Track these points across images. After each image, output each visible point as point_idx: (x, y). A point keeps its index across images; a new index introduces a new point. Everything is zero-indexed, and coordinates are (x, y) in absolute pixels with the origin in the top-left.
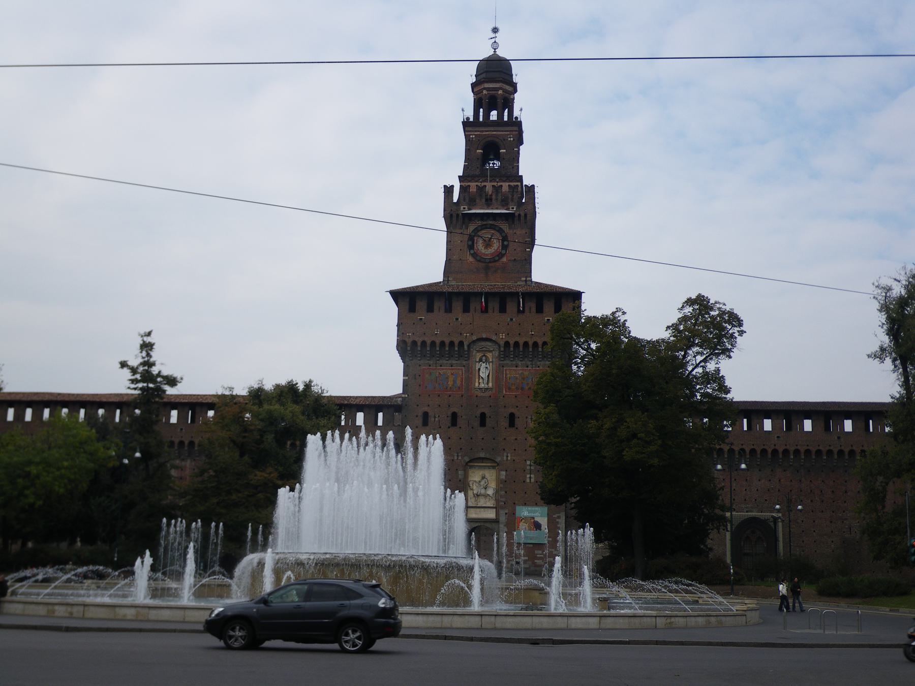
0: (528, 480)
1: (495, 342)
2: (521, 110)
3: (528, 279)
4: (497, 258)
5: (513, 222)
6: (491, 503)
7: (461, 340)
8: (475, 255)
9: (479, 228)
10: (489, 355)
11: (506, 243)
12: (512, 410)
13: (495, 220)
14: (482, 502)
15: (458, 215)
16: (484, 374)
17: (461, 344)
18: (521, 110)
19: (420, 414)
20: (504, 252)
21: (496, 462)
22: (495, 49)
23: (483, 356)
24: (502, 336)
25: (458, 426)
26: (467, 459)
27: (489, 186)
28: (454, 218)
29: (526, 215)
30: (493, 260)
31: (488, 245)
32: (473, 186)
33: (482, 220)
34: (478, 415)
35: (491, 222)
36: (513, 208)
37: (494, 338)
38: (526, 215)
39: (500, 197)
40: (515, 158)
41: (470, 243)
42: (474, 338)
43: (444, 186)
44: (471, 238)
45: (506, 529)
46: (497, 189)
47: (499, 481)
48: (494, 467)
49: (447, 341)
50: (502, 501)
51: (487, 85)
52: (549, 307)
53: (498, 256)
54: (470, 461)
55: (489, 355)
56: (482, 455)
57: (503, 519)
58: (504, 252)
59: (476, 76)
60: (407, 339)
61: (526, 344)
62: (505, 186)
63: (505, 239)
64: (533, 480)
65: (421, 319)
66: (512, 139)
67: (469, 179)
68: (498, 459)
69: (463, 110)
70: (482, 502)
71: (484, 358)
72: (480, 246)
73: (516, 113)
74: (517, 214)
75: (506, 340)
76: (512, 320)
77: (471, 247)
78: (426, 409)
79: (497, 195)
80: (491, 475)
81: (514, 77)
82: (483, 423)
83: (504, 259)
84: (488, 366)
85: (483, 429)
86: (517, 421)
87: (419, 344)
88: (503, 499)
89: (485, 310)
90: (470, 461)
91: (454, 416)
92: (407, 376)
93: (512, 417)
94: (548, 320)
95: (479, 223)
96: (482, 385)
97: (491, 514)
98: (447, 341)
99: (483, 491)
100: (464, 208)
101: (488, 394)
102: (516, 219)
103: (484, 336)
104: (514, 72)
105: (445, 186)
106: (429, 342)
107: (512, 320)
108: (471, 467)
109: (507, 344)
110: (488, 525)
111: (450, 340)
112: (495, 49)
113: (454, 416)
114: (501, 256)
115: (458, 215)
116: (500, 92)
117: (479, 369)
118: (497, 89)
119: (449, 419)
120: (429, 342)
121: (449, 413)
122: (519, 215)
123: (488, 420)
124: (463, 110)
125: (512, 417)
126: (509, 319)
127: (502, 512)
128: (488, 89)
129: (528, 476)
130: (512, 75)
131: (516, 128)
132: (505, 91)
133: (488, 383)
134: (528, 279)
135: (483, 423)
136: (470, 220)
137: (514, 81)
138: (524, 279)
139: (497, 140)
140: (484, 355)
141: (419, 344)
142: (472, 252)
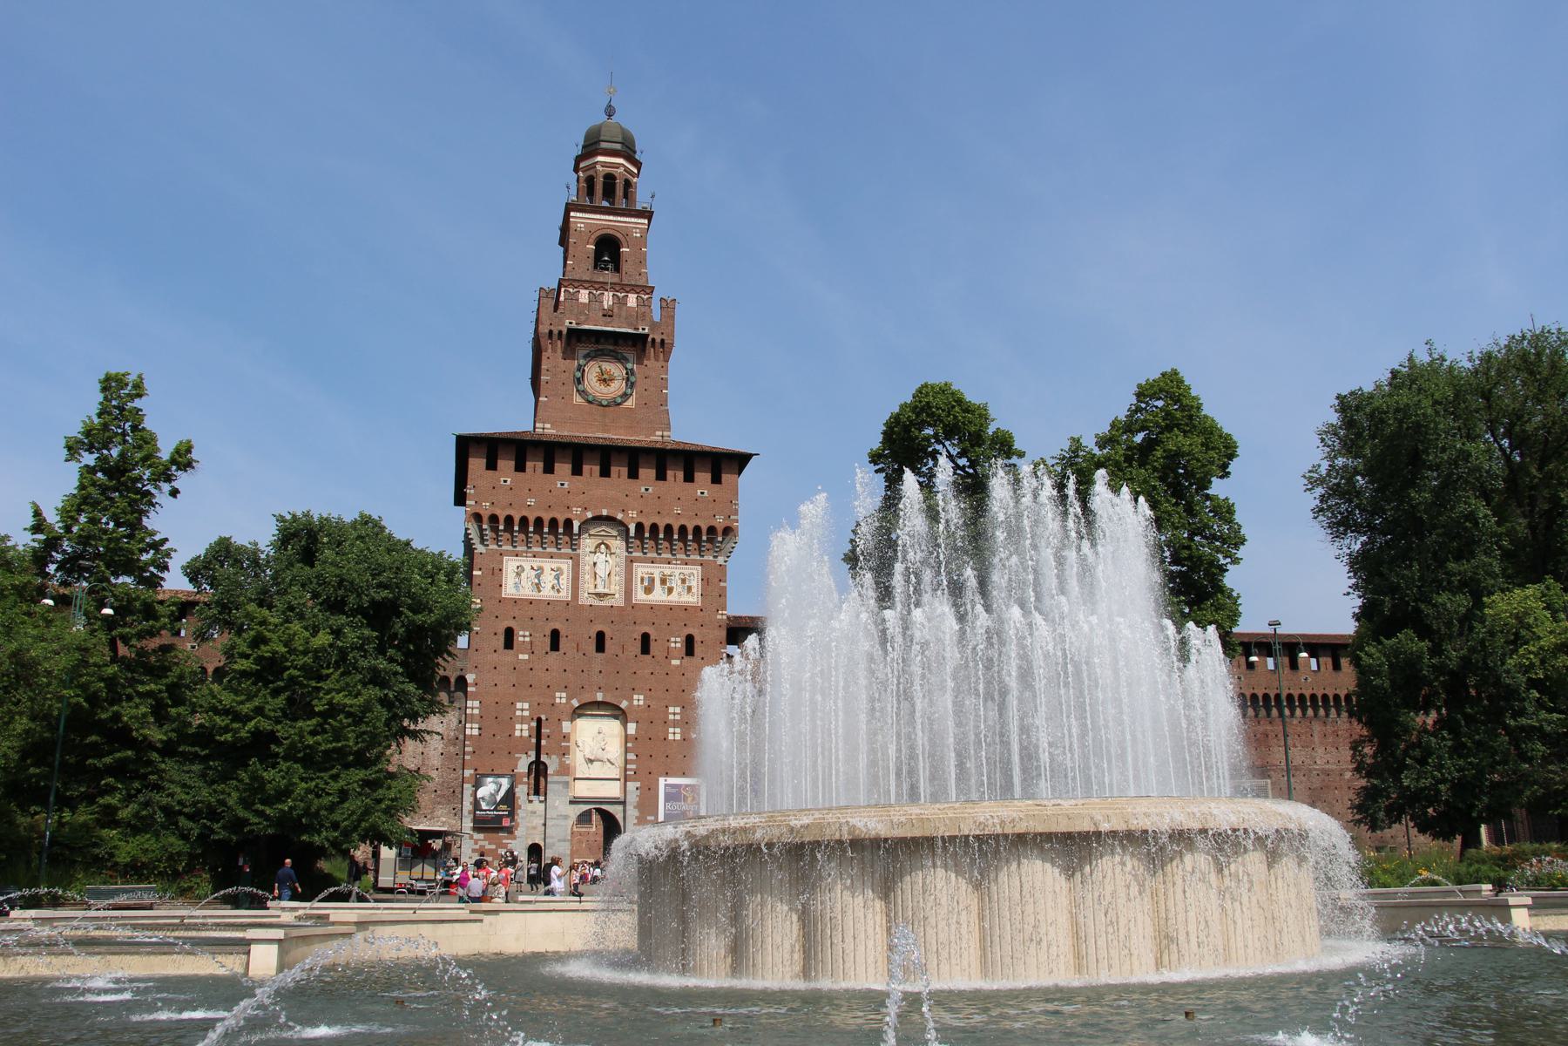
0: (671, 737)
1: (622, 526)
2: (653, 197)
3: (665, 433)
4: (619, 400)
5: (644, 350)
6: (615, 772)
7: (569, 516)
8: (583, 393)
9: (593, 354)
10: (611, 542)
11: (632, 379)
12: (646, 629)
13: (616, 344)
14: (596, 770)
15: (560, 332)
16: (602, 570)
17: (568, 523)
18: (653, 197)
19: (501, 632)
20: (629, 391)
21: (620, 709)
22: (610, 116)
23: (600, 544)
24: (633, 514)
25: (562, 651)
26: (577, 705)
27: (608, 299)
28: (555, 337)
29: (663, 341)
30: (615, 403)
31: (605, 380)
32: (584, 296)
33: (597, 342)
34: (594, 636)
35: (611, 348)
36: (643, 329)
37: (620, 516)
38: (663, 341)
39: (624, 314)
40: (642, 262)
41: (579, 374)
42: (589, 515)
43: (541, 288)
44: (580, 368)
45: (636, 813)
46: (622, 302)
47: (627, 738)
48: (616, 717)
49: (546, 518)
50: (631, 770)
51: (600, 158)
52: (703, 477)
53: (621, 396)
54: (582, 706)
55: (611, 542)
56: (600, 697)
57: (633, 798)
58: (629, 391)
59: (584, 147)
60: (481, 512)
61: (669, 528)
62: (632, 300)
63: (630, 372)
64: (678, 737)
65: (505, 481)
66: (638, 235)
67: (576, 284)
68: (624, 705)
69: (568, 187)
70: (596, 770)
71: (603, 546)
72: (592, 382)
73: (641, 201)
74: (650, 339)
75: (639, 520)
76: (647, 490)
77: (579, 381)
78: (512, 624)
79: (619, 308)
80: (613, 726)
81: (638, 153)
82: (600, 646)
83: (630, 403)
84: (608, 558)
85: (600, 654)
86: (652, 644)
87: (502, 520)
88: (634, 767)
89: (605, 473)
90: (577, 708)
91: (555, 635)
92: (480, 569)
93: (645, 639)
94: (702, 493)
95: (595, 347)
96: (600, 590)
97: (613, 790)
98: (546, 518)
99: (600, 754)
100: (571, 323)
101: (606, 603)
102: (649, 345)
103: (605, 513)
104: (637, 148)
105: (541, 288)
106: (517, 520)
107: (647, 490)
108: (580, 716)
109: (639, 527)
110: (604, 807)
111: (551, 516)
112: (610, 116)
113: (555, 635)
114: (625, 396)
115: (560, 332)
116: (622, 169)
117: (595, 564)
118: (618, 166)
119: (548, 640)
120: (517, 520)
121: (548, 633)
122: (653, 340)
123: (608, 643)
124: (568, 187)
125: (645, 639)
126: (643, 489)
127: (631, 786)
128: (604, 165)
129: (671, 730)
130: (635, 152)
131: (646, 221)
132: (627, 170)
133: (609, 588)
134: (665, 433)
135: (600, 646)
136: (579, 341)
137: (637, 157)
138: (660, 433)
139: (618, 235)
140: (603, 543)
141: (502, 520)
142: (580, 387)
